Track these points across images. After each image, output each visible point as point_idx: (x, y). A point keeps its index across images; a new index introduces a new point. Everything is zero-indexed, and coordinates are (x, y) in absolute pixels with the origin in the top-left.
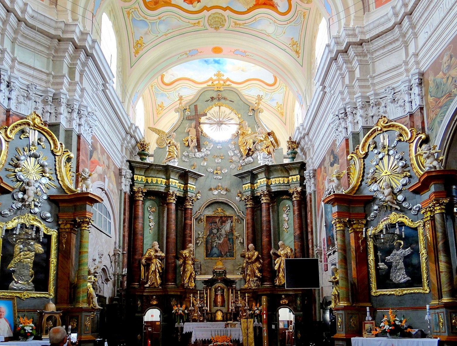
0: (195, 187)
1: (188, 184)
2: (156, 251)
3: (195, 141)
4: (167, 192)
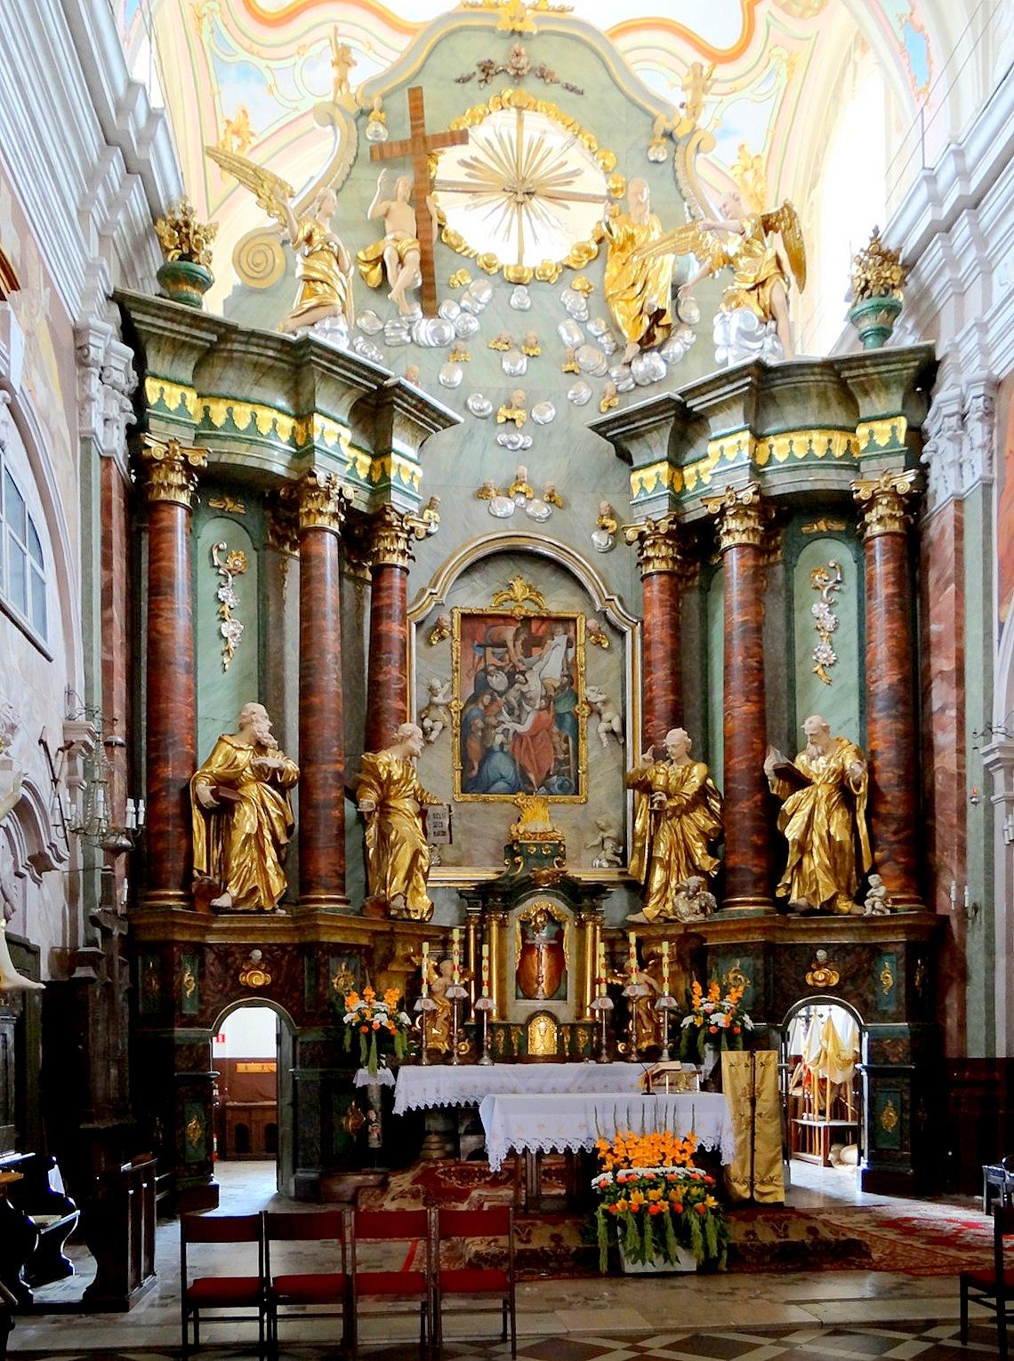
0: (419, 472)
1: (388, 451)
2: (260, 748)
3: (413, 258)
4: (302, 480)
